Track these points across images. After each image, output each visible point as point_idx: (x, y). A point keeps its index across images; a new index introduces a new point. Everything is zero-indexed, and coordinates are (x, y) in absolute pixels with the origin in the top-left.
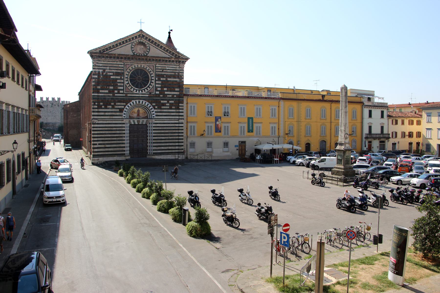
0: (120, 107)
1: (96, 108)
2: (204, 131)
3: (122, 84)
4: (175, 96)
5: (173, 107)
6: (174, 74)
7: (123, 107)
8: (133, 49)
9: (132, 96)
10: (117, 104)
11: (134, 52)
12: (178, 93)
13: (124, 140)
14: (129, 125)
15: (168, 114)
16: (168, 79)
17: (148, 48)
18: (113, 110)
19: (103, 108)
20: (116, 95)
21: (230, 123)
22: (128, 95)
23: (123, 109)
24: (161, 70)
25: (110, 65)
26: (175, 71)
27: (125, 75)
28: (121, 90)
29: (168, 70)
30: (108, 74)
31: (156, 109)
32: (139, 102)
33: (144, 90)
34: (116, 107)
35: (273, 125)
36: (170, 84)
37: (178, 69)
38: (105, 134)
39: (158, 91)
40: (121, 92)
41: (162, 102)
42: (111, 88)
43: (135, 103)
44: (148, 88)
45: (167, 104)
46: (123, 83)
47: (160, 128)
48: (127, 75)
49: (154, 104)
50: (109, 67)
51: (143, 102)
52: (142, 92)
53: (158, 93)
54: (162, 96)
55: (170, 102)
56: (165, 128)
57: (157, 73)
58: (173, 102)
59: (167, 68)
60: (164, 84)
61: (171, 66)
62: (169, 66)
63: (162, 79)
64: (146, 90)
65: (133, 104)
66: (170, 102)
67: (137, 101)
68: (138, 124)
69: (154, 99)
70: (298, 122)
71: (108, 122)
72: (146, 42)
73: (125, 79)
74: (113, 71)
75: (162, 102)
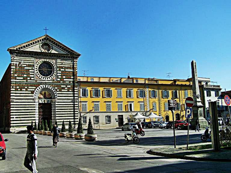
0: (31, 90)
1: (14, 91)
2: (93, 107)
3: (33, 73)
4: (71, 82)
5: (70, 90)
6: (70, 66)
7: (34, 90)
8: (41, 48)
9: (40, 82)
10: (29, 87)
11: (41, 50)
12: (72, 80)
13: (35, 115)
15: (66, 95)
16: (66, 70)
17: (52, 47)
19: (19, 91)
20: (29, 81)
22: (38, 81)
23: (34, 91)
24: (61, 64)
25: (24, 59)
28: (32, 77)
30: (23, 65)
31: (58, 91)
32: (46, 86)
33: (49, 77)
34: (28, 90)
36: (67, 74)
38: (21, 110)
39: (59, 78)
40: (32, 79)
41: (62, 86)
43: (42, 87)
44: (52, 76)
45: (66, 88)
48: (36, 66)
50: (23, 60)
52: (47, 79)
53: (59, 79)
54: (61, 82)
55: (68, 86)
57: (58, 65)
58: (70, 86)
60: (63, 73)
63: (61, 70)
64: (50, 77)
65: (42, 88)
66: (68, 86)
71: (22, 101)
72: (50, 43)
73: (35, 70)
75: (62, 86)
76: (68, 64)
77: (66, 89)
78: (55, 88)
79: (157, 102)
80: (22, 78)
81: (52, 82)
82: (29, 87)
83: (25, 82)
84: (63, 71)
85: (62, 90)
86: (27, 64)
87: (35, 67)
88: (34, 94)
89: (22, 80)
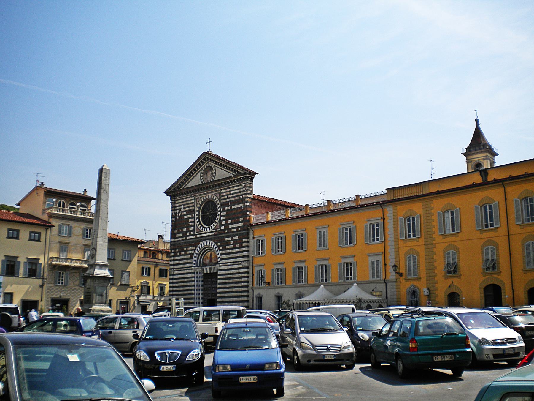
0: (191, 252)
5: (238, 246)
7: (193, 252)
14: (202, 275)
15: (232, 255)
16: (233, 207)
18: (186, 257)
20: (188, 238)
21: (305, 261)
22: (198, 236)
23: (193, 254)
24: (226, 197)
25: (184, 203)
26: (239, 194)
28: (192, 231)
29: (233, 194)
32: (207, 242)
34: (188, 253)
35: (375, 259)
37: (242, 190)
40: (192, 233)
41: (227, 239)
42: (185, 230)
46: (194, 222)
47: (225, 277)
48: (197, 211)
49: (219, 244)
53: (223, 228)
54: (226, 231)
55: (235, 238)
56: (229, 276)
57: (222, 201)
59: (232, 192)
61: (235, 188)
62: (233, 189)
66: (235, 238)
67: (205, 242)
68: (210, 273)
70: (429, 245)
75: (227, 239)
79: (421, 250)
80: (181, 235)
89: (181, 237)
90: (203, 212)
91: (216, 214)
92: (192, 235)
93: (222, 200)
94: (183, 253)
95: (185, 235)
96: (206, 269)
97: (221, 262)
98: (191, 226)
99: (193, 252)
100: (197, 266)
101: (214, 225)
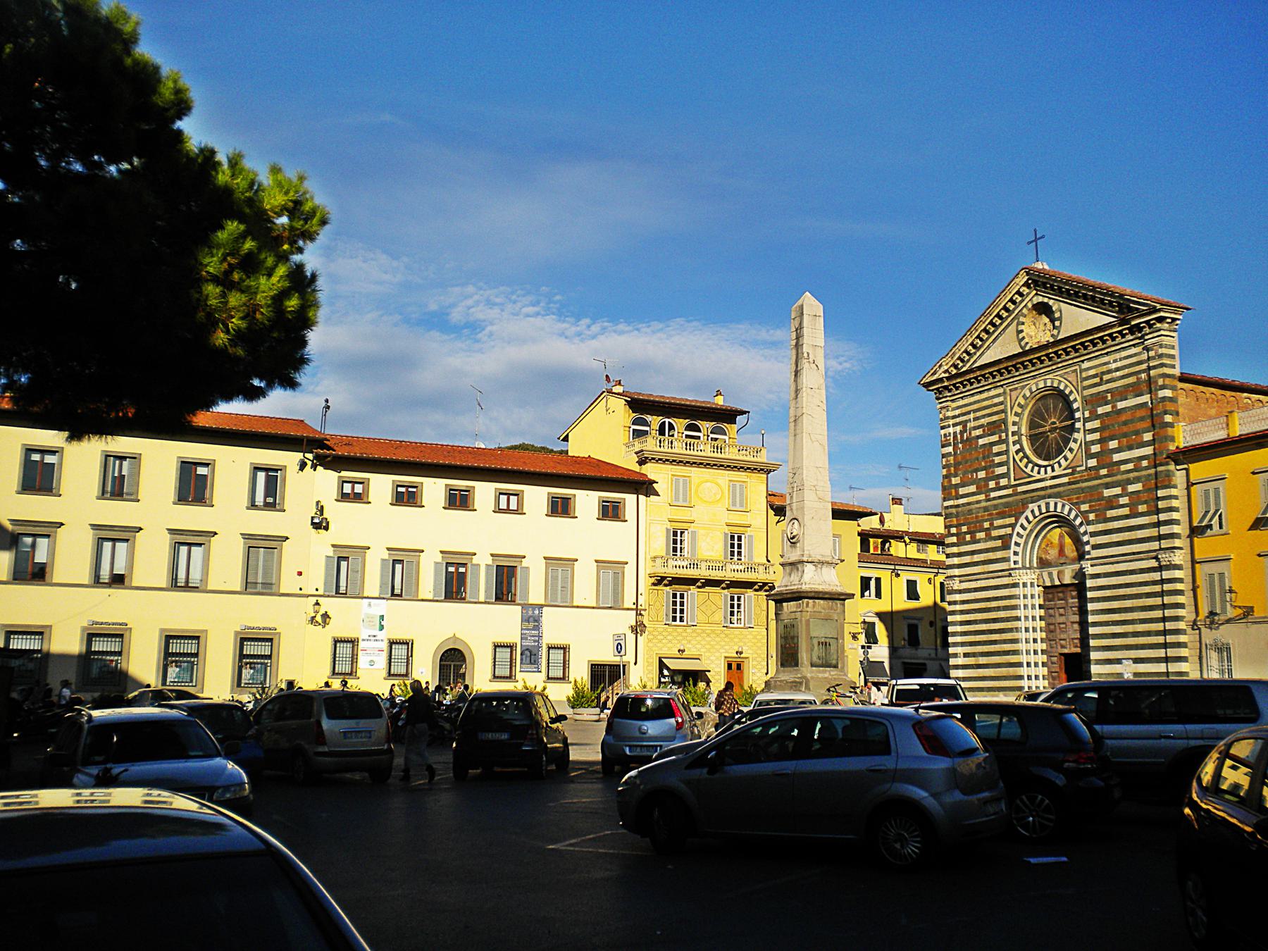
0: (1002, 532)
1: (953, 545)
3: (1004, 458)
4: (1145, 463)
7: (1009, 530)
12: (1148, 451)
16: (1121, 405)
20: (993, 495)
22: (1020, 489)
23: (1011, 535)
24: (1097, 380)
27: (1010, 424)
29: (1117, 369)
32: (1048, 504)
34: (995, 533)
36: (1125, 423)
40: (1003, 482)
41: (1107, 493)
42: (982, 474)
48: (1014, 424)
49: (1085, 507)
50: (975, 411)
51: (1056, 504)
52: (1053, 470)
53: (1093, 463)
54: (1104, 472)
55: (1131, 488)
57: (1086, 393)
58: (1137, 487)
59: (1114, 366)
61: (1124, 354)
62: (1117, 356)
63: (1100, 410)
66: (1131, 488)
67: (1042, 503)
69: (1082, 489)
73: (1011, 439)
74: (982, 421)
75: (1107, 493)
76: (1126, 371)
77: (1123, 506)
78: (1079, 509)
80: (973, 489)
81: (1065, 480)
82: (997, 523)
83: (984, 504)
84: (1107, 414)
85: (1110, 513)
86: (982, 426)
87: (1012, 429)
88: (1009, 548)
89: (973, 494)
90: (1033, 424)
91: (1072, 429)
92: (1005, 487)
93: (1085, 388)
94: (981, 535)
95: (982, 488)
96: (1050, 574)
97: (1095, 553)
98: (1000, 465)
99: (1009, 530)
100: (1024, 567)
101: (1066, 459)
